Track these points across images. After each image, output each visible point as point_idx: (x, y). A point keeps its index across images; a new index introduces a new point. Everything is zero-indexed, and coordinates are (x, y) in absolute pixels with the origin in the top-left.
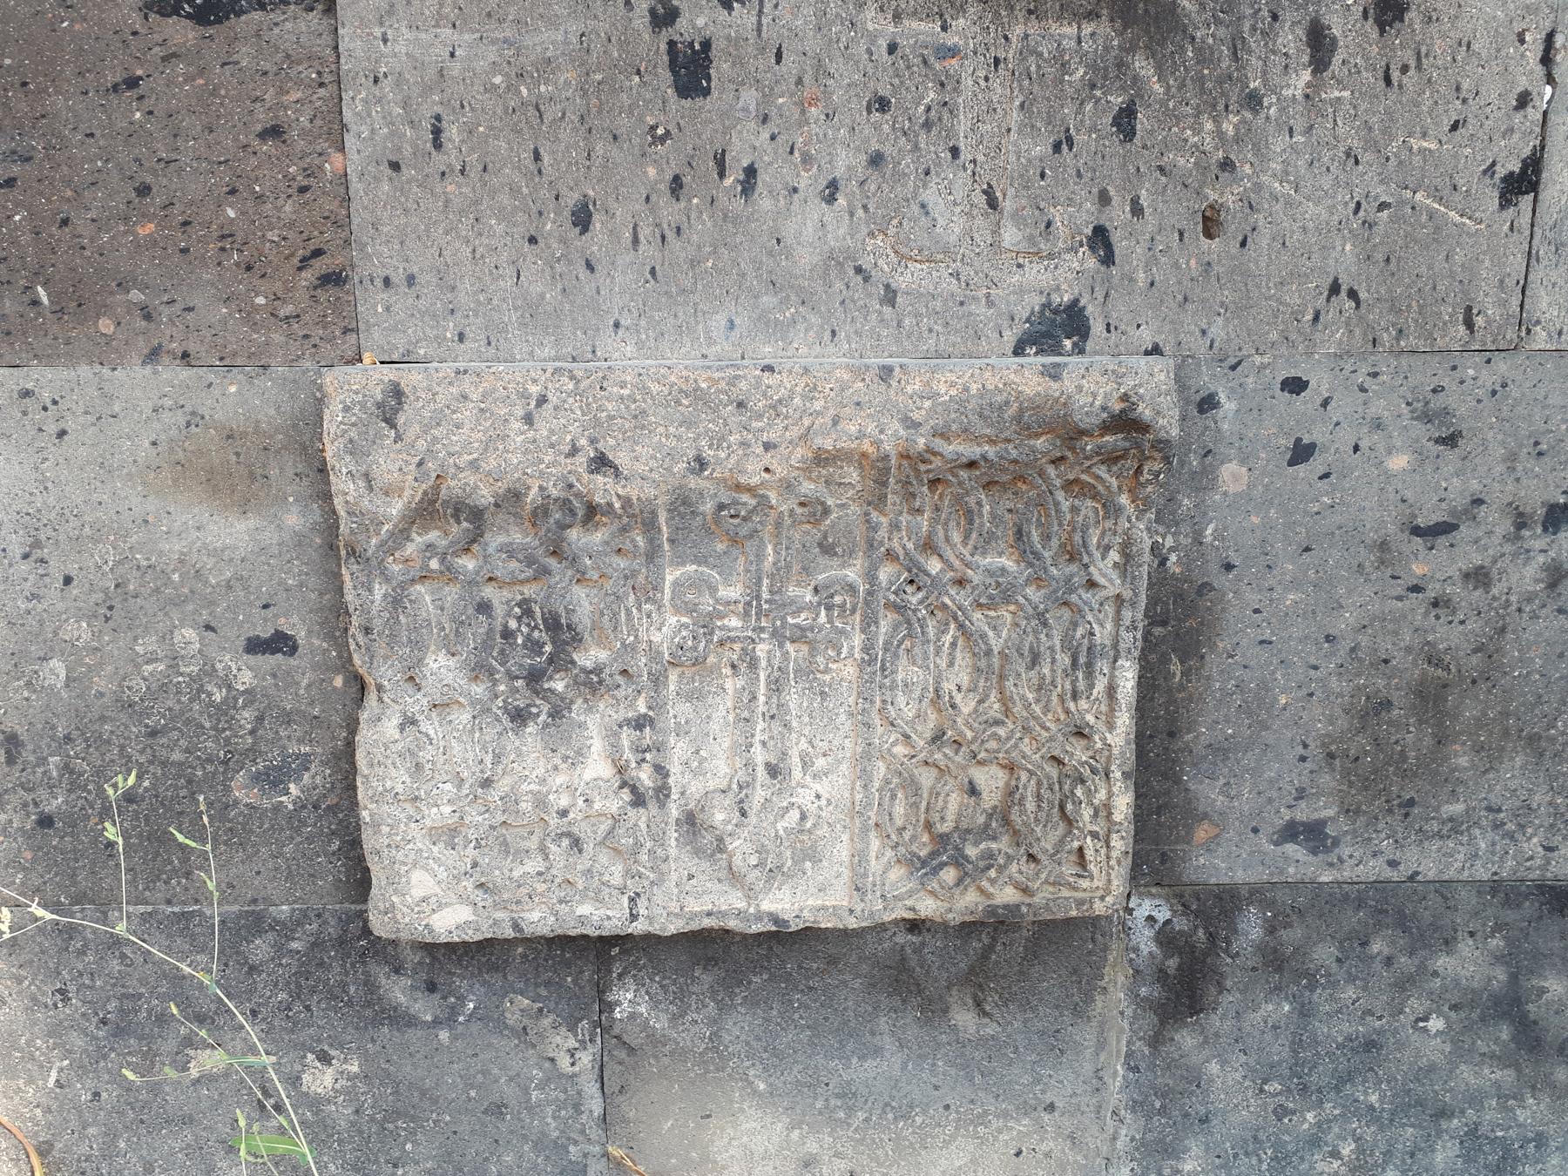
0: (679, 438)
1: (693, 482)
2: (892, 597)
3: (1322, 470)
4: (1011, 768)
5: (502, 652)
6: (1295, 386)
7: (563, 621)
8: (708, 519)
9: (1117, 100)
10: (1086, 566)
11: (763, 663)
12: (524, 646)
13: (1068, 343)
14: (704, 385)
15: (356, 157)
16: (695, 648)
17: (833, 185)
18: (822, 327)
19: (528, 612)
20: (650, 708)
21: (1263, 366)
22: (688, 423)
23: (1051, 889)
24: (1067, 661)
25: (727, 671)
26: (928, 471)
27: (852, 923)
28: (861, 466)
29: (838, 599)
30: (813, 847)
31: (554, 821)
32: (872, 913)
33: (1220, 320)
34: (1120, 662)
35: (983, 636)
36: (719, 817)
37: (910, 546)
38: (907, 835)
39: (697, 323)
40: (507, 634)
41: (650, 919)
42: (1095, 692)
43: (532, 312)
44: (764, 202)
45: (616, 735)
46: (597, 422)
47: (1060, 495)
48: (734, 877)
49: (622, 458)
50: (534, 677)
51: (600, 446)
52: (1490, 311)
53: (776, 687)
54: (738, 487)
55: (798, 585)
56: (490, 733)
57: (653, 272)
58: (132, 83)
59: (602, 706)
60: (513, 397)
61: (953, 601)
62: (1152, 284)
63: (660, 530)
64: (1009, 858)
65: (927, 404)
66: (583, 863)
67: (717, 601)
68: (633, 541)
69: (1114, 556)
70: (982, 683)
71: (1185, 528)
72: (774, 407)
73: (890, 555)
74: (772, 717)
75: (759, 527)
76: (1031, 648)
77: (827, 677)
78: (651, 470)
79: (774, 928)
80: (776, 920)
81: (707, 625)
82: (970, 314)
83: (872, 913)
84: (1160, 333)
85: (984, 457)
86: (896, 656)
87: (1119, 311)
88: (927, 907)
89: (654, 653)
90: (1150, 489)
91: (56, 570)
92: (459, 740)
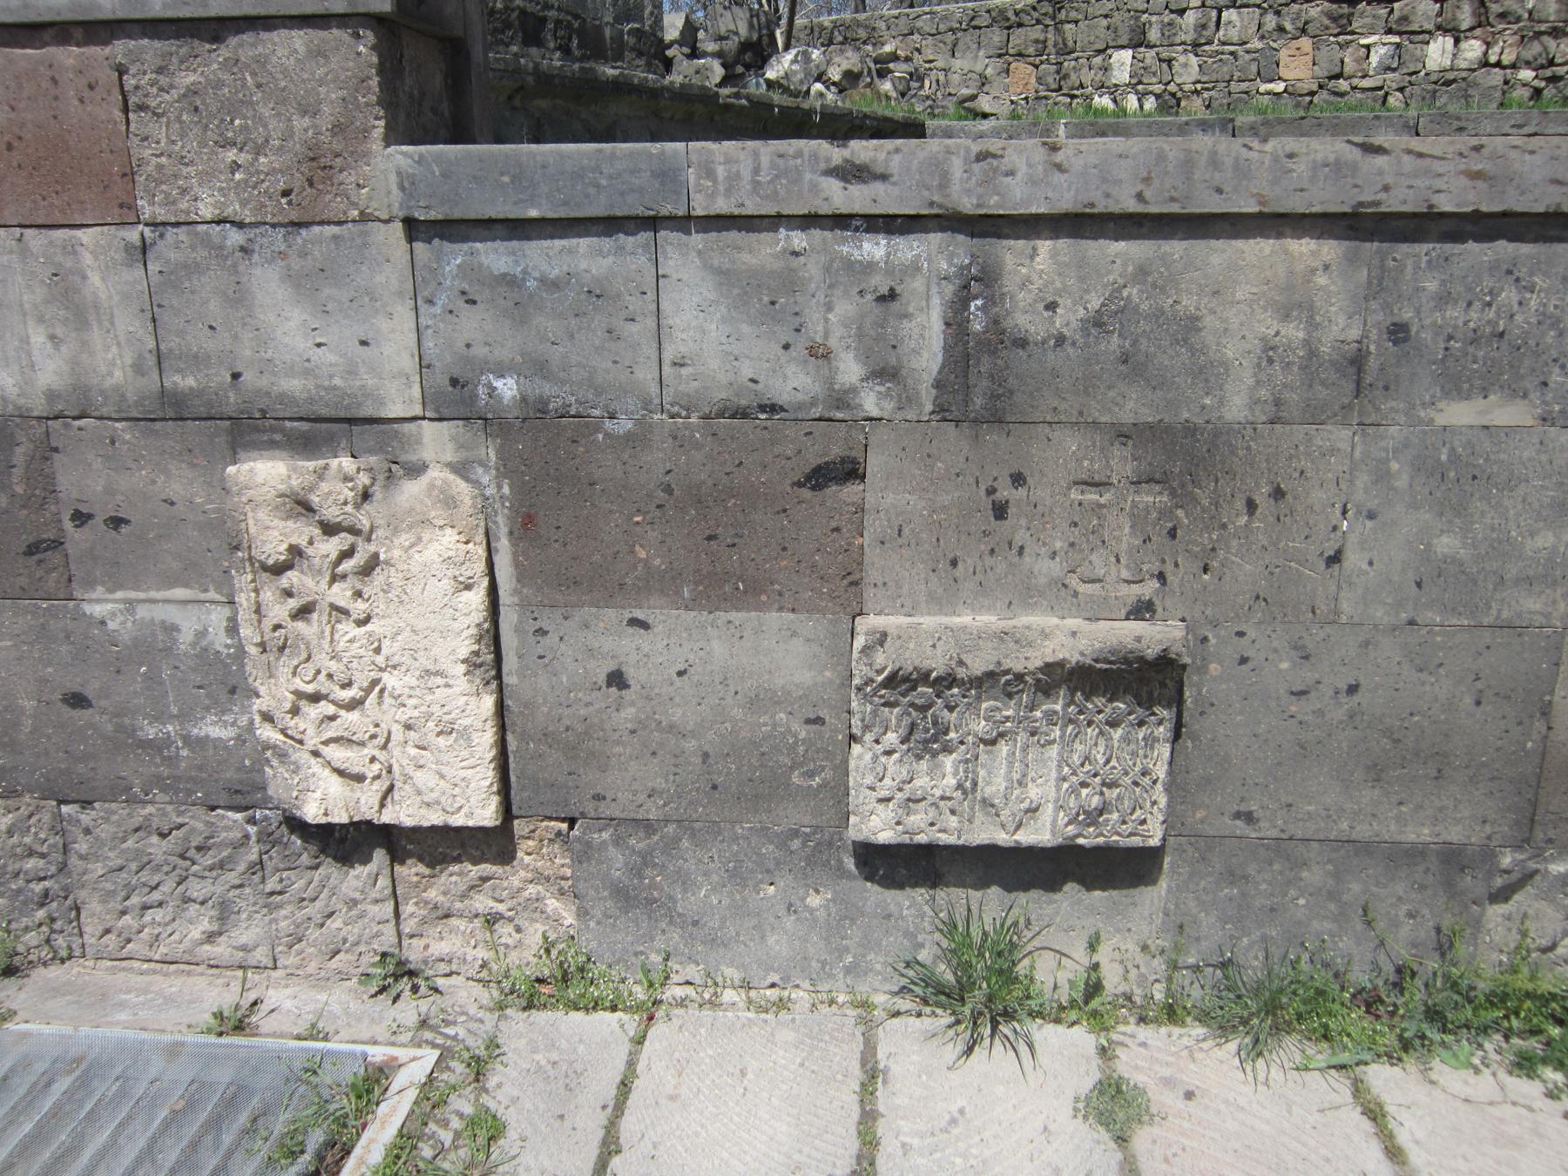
6: (1241, 634)
9: (1170, 525)
15: (867, 540)
17: (1054, 553)
44: (1027, 559)
49: (969, 662)
52: (1322, 608)
53: (1025, 749)
58: (785, 511)
87: (1168, 603)
91: (732, 689)
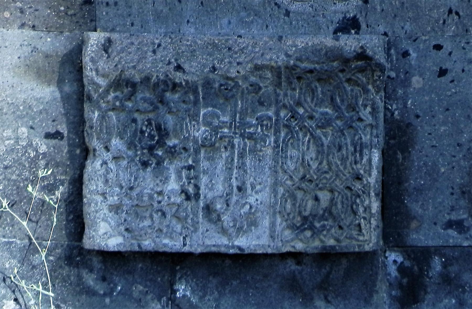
0: (207, 60)
1: (211, 76)
2: (285, 122)
3: (450, 79)
4: (332, 191)
5: (140, 139)
7: (163, 127)
8: (217, 91)
10: (358, 112)
11: (237, 146)
12: (148, 137)
13: (353, 32)
14: (217, 42)
16: (211, 139)
18: (263, 24)
19: (150, 124)
20: (193, 162)
21: (426, 40)
22: (210, 54)
23: (348, 241)
24: (353, 149)
25: (223, 150)
26: (296, 74)
27: (270, 251)
28: (272, 72)
29: (265, 123)
30: (255, 220)
31: (155, 205)
32: (277, 247)
33: (408, 24)
34: (373, 150)
35: (320, 138)
36: (219, 206)
37: (292, 102)
38: (291, 216)
39: (217, 21)
40: (142, 132)
41: (191, 246)
42: (363, 161)
43: (158, 16)
45: (180, 172)
46: (178, 54)
47: (346, 85)
48: (224, 231)
49: (186, 67)
50: (151, 149)
51: (179, 62)
53: (242, 156)
54: (228, 78)
55: (251, 117)
56: (134, 169)
57: (202, 3)
59: (175, 162)
60: (149, 44)
61: (308, 124)
62: (383, 10)
63: (199, 93)
64: (331, 227)
65: (294, 49)
66: (166, 222)
67: (220, 122)
68: (189, 97)
69: (369, 109)
70: (320, 157)
71: (400, 102)
72: (241, 50)
73: (285, 106)
74: (240, 168)
75: (235, 93)
76: (339, 145)
77: (261, 154)
78: (196, 71)
79: (239, 252)
80: (239, 248)
81: (215, 130)
82: (317, 20)
83: (277, 247)
84: (386, 28)
85: (315, 68)
86: (287, 145)
87: (371, 19)
88: (300, 246)
89: (195, 141)
90: (378, 82)
92: (122, 171)
